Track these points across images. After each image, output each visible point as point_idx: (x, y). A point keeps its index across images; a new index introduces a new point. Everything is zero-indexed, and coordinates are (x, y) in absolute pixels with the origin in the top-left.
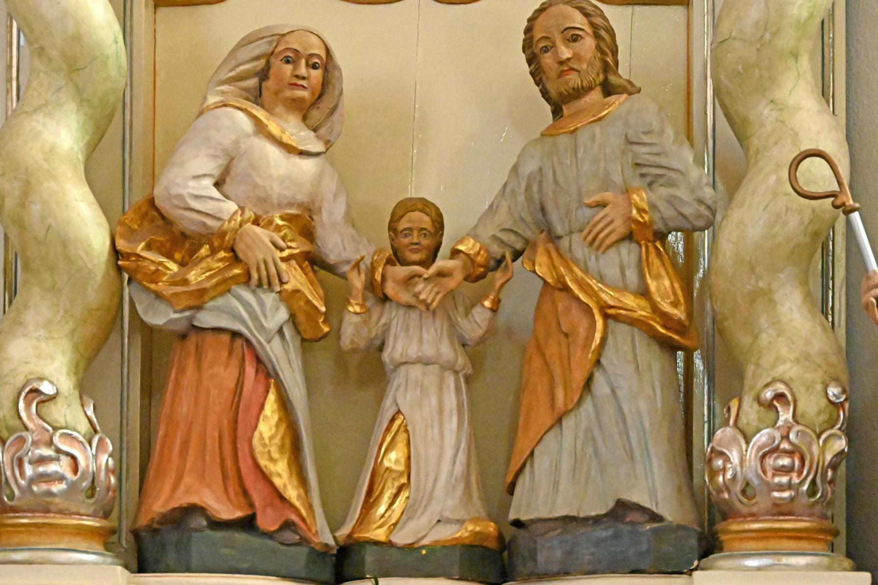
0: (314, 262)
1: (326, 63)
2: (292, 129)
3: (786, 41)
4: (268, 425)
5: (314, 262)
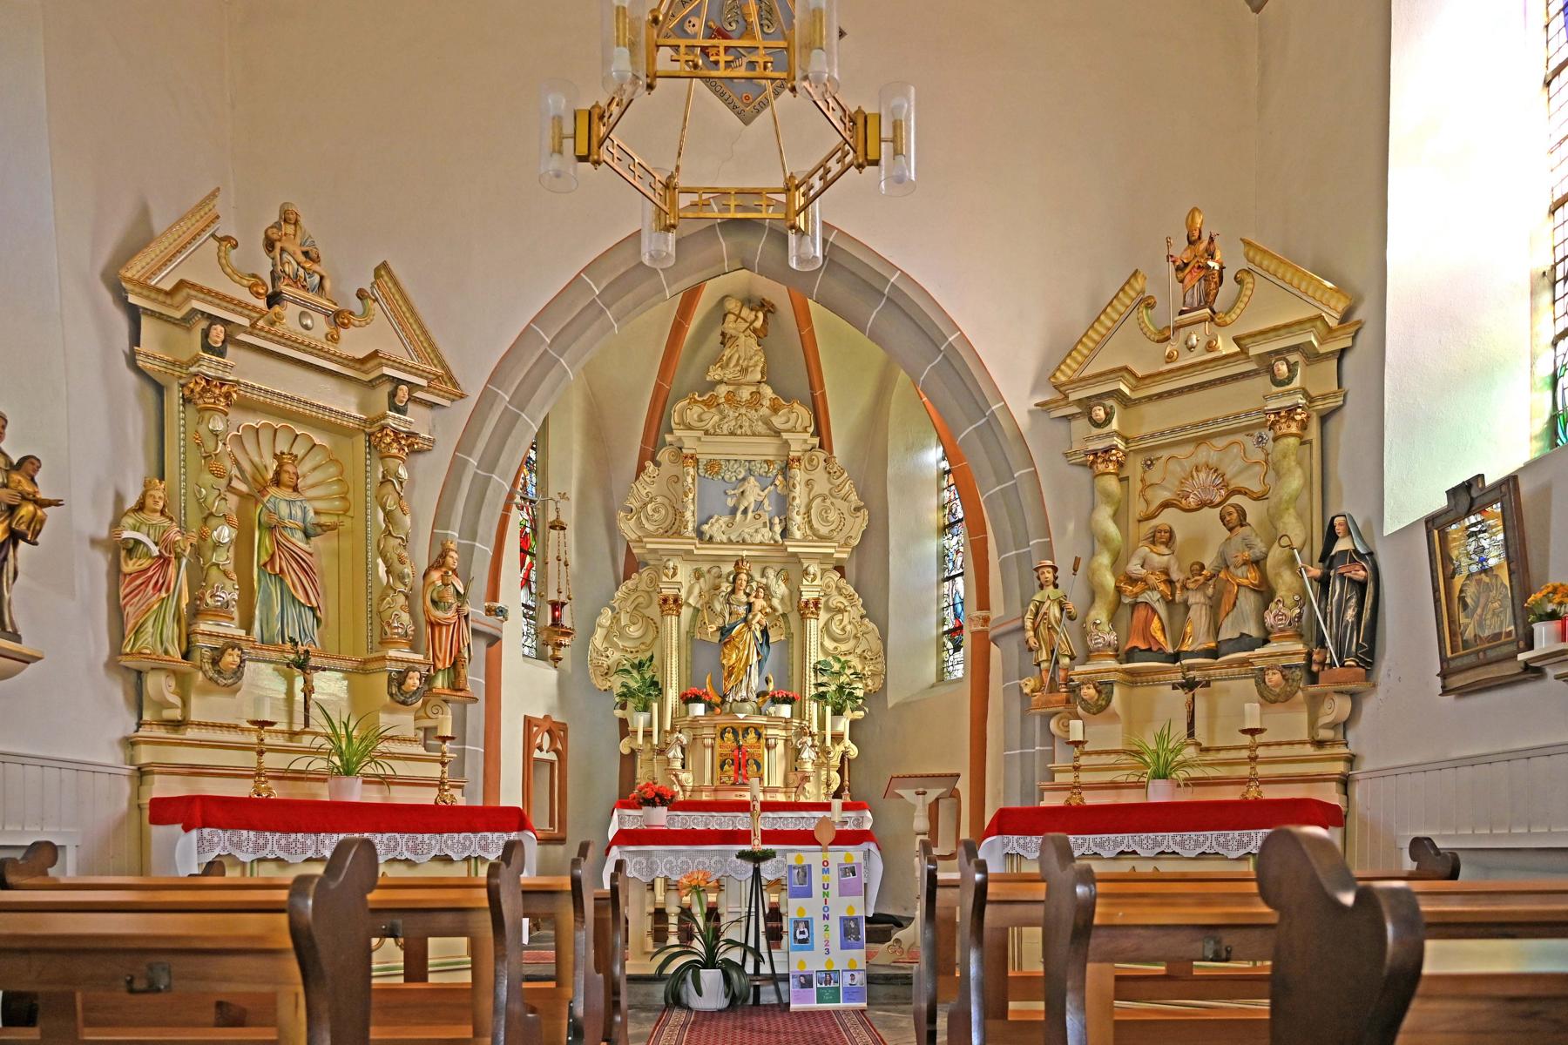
0: (1170, 582)
1: (1171, 532)
2: (1163, 549)
3: (1283, 506)
4: (1156, 624)
5: (1170, 582)
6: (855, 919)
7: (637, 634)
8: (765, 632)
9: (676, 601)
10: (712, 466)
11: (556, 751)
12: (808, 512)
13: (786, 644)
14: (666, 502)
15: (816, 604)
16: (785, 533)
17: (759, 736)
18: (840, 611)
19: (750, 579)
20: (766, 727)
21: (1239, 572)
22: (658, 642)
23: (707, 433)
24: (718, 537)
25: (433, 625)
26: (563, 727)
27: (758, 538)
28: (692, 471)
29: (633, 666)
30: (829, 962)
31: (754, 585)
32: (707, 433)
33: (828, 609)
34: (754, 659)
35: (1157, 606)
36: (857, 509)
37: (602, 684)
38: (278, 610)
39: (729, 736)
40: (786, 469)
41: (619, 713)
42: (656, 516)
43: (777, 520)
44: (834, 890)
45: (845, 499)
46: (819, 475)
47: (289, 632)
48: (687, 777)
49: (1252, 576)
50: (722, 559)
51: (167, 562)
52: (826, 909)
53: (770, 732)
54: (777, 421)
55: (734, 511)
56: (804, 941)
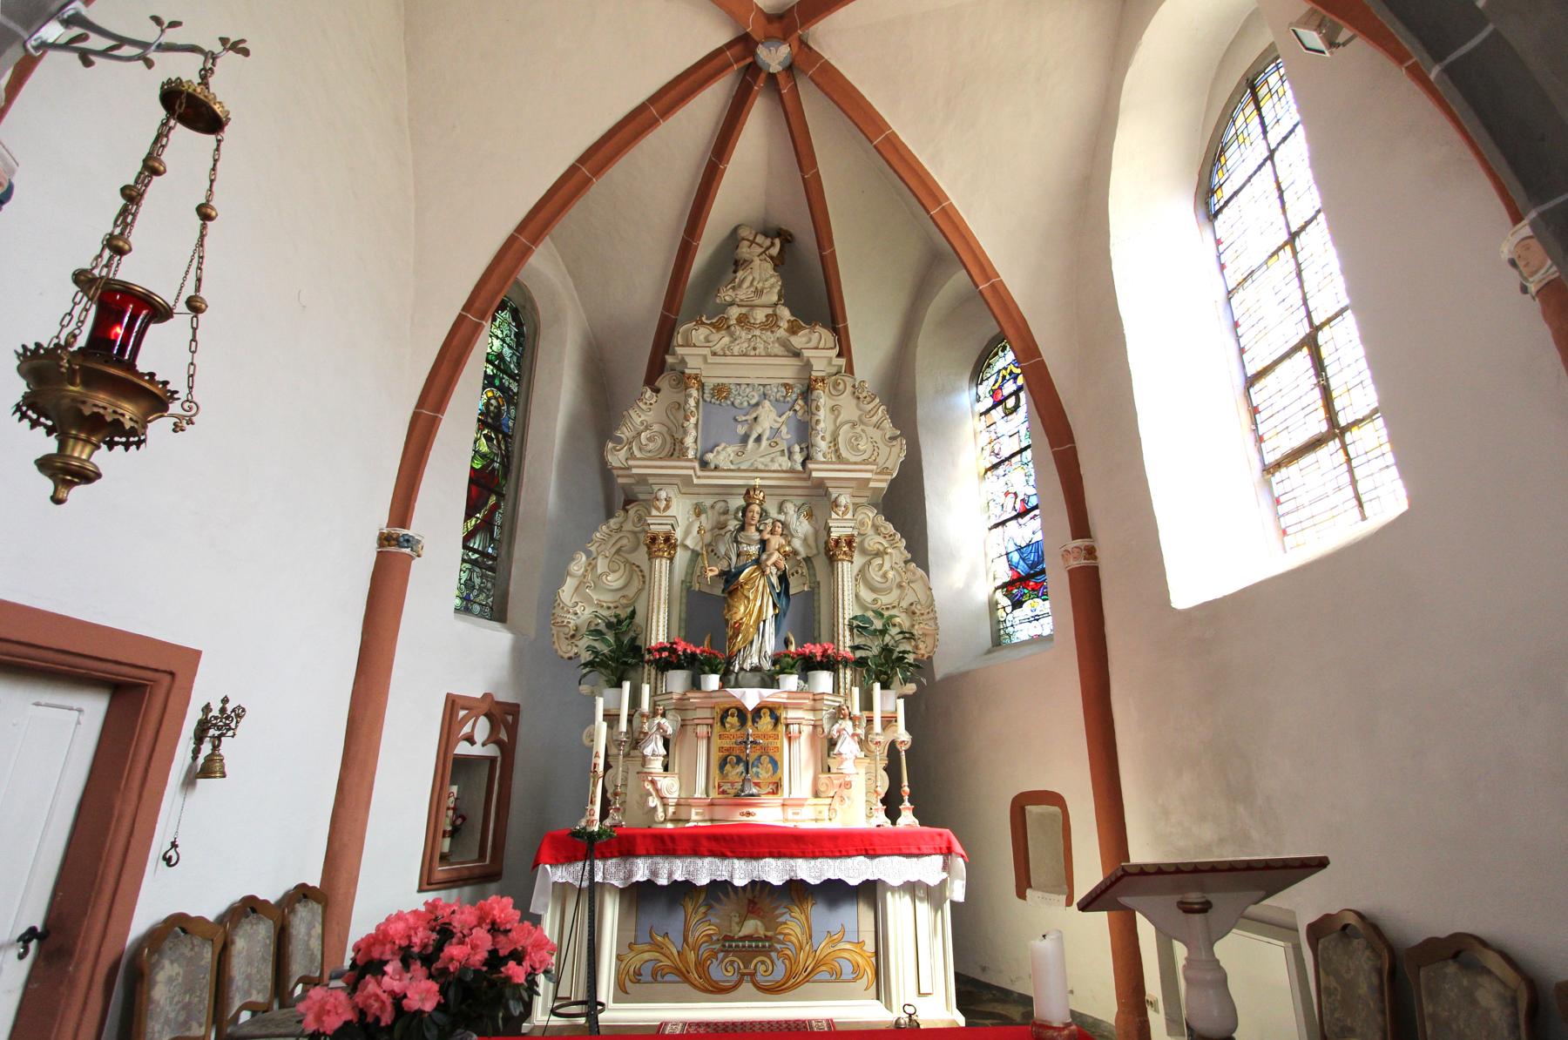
8: (783, 578)
9: (667, 539)
10: (721, 391)
11: (499, 743)
12: (835, 440)
13: (811, 597)
14: (664, 430)
15: (850, 543)
17: (777, 720)
18: (878, 554)
19: (764, 514)
20: (785, 707)
22: (644, 595)
23: (714, 354)
26: (514, 709)
27: (775, 467)
28: (694, 393)
29: (609, 625)
31: (769, 521)
32: (714, 354)
33: (864, 552)
36: (893, 438)
39: (732, 720)
40: (807, 393)
42: (650, 440)
43: (797, 448)
45: (877, 426)
46: (846, 400)
48: (670, 785)
50: (727, 490)
53: (791, 714)
54: (797, 341)
55: (744, 439)
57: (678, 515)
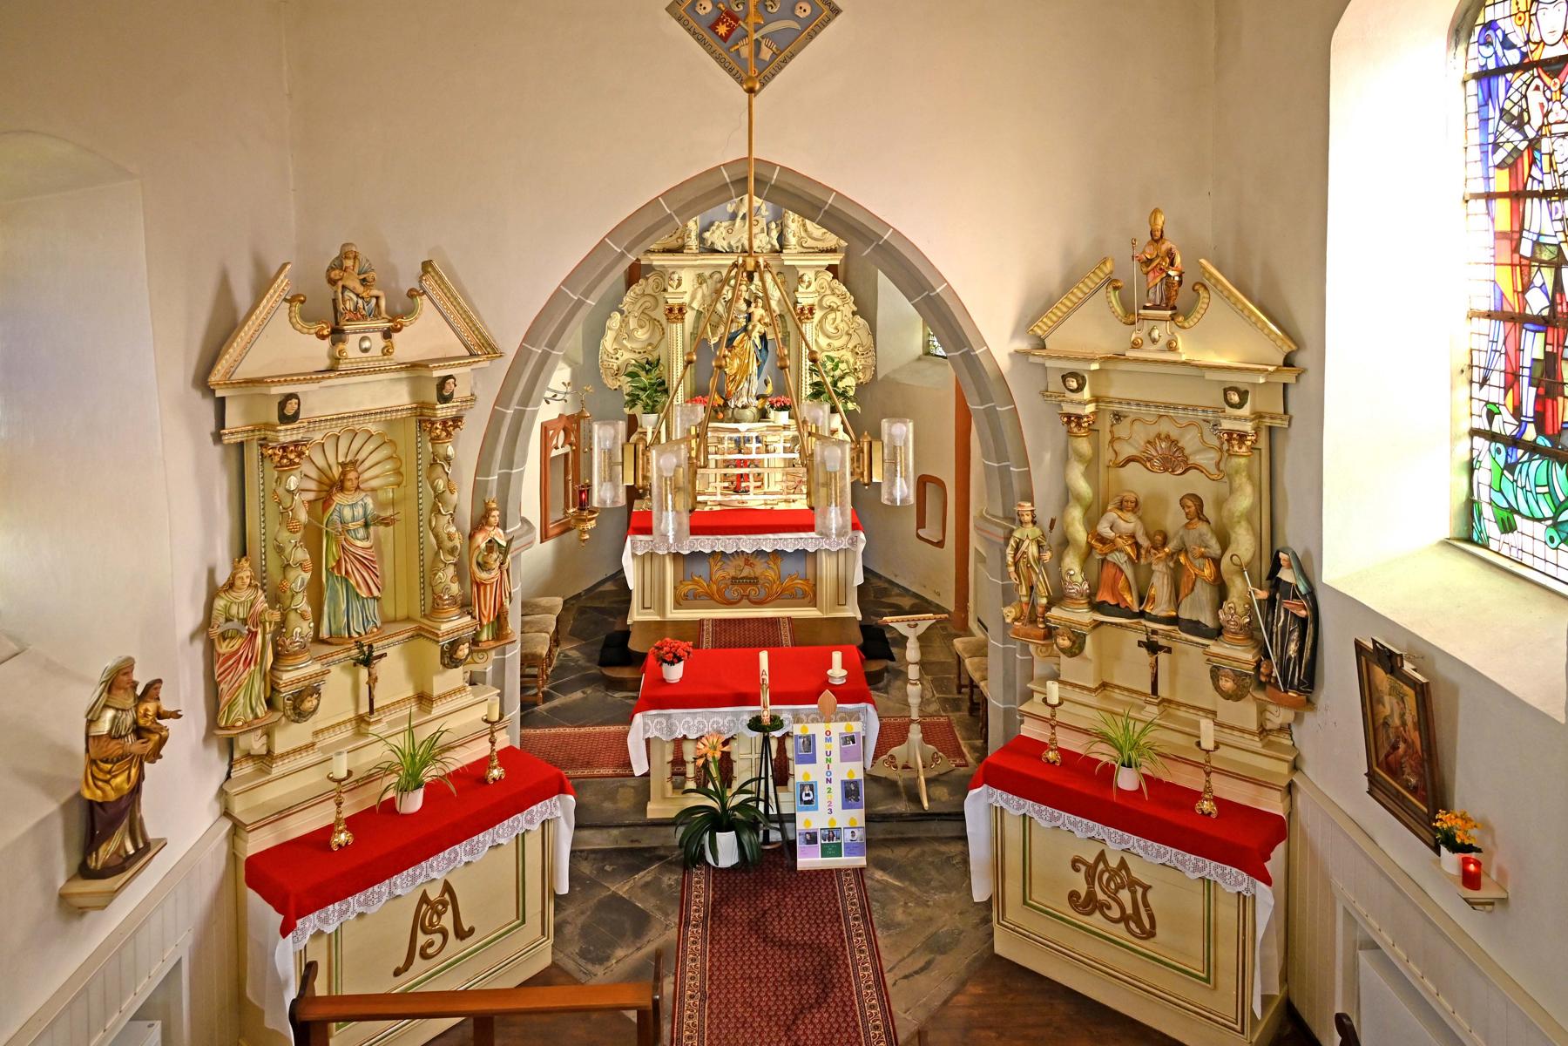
0: (1137, 546)
4: (1121, 583)
5: (1137, 546)
6: (855, 783)
7: (644, 337)
8: (763, 337)
16: (781, 237)
21: (1197, 562)
24: (720, 244)
25: (478, 585)
30: (832, 820)
34: (754, 368)
35: (1124, 567)
37: (612, 383)
38: (344, 607)
41: (627, 410)
44: (836, 756)
47: (357, 626)
49: (1208, 572)
51: (254, 635)
52: (829, 773)
56: (810, 802)
57: (687, 288)
